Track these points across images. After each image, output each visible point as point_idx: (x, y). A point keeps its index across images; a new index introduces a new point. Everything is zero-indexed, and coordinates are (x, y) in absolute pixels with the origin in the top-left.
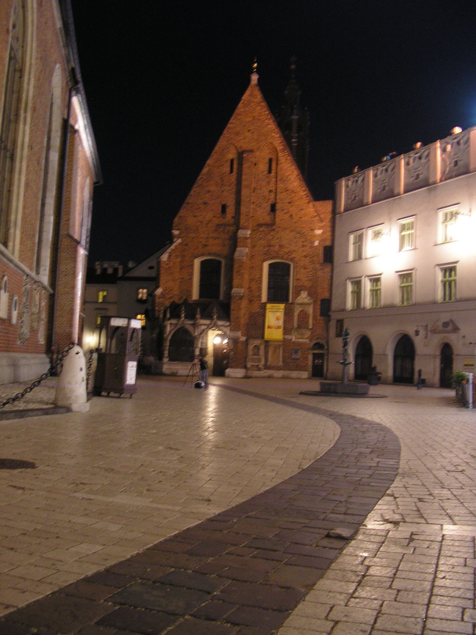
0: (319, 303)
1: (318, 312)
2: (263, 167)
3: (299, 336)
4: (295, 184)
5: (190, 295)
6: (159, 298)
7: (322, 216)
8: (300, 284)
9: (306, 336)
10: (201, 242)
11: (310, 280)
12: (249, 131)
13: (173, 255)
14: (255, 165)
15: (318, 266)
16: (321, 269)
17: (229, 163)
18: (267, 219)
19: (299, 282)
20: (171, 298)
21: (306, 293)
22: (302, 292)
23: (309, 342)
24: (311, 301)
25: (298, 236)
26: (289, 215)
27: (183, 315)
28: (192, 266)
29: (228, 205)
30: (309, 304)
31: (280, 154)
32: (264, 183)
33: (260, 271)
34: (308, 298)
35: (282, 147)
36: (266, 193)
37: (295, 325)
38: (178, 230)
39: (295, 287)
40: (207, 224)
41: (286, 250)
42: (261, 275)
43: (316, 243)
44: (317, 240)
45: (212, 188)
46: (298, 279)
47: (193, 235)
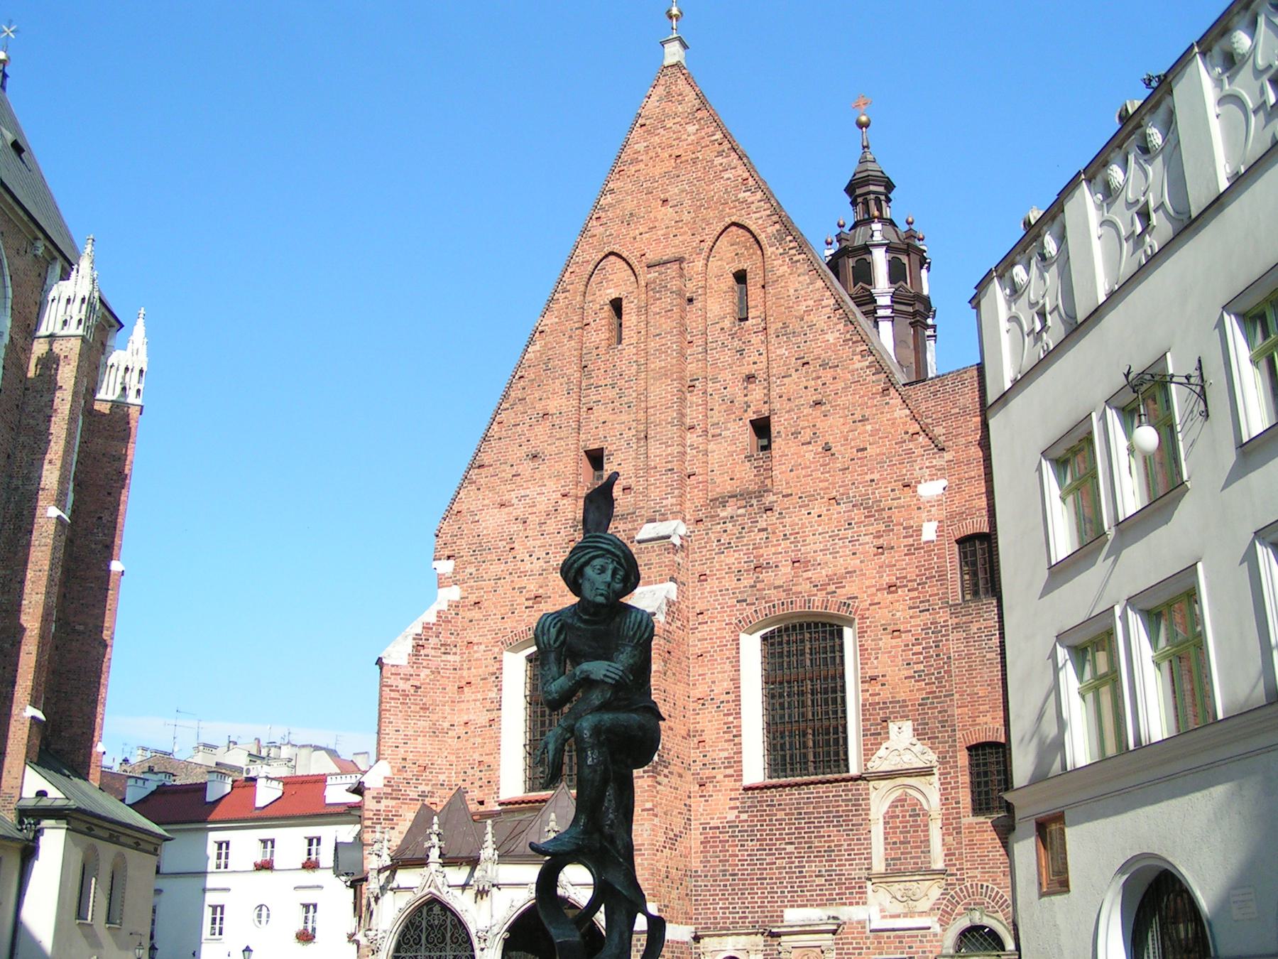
0: (963, 759)
1: (965, 797)
2: (719, 304)
3: (898, 908)
4: (831, 338)
5: (491, 783)
6: (378, 799)
7: (939, 431)
8: (886, 694)
9: (924, 905)
10: (521, 589)
11: (918, 676)
12: (665, 201)
13: (433, 641)
14: (690, 300)
15: (943, 616)
16: (956, 627)
17: (608, 311)
18: (746, 475)
19: (878, 689)
20: (423, 795)
21: (908, 726)
22: (893, 727)
23: (937, 928)
24: (932, 757)
25: (858, 515)
26: (821, 442)
27: (434, 853)
28: (497, 675)
29: (606, 453)
30: (926, 772)
31: (769, 251)
32: (727, 357)
33: (728, 667)
34: (919, 747)
35: (772, 230)
36: (737, 390)
37: (879, 866)
38: (449, 557)
39: (865, 708)
40: (541, 524)
41: (820, 574)
42: (736, 681)
43: (929, 532)
44: (929, 520)
45: (553, 406)
46: (873, 679)
47: (497, 569)
